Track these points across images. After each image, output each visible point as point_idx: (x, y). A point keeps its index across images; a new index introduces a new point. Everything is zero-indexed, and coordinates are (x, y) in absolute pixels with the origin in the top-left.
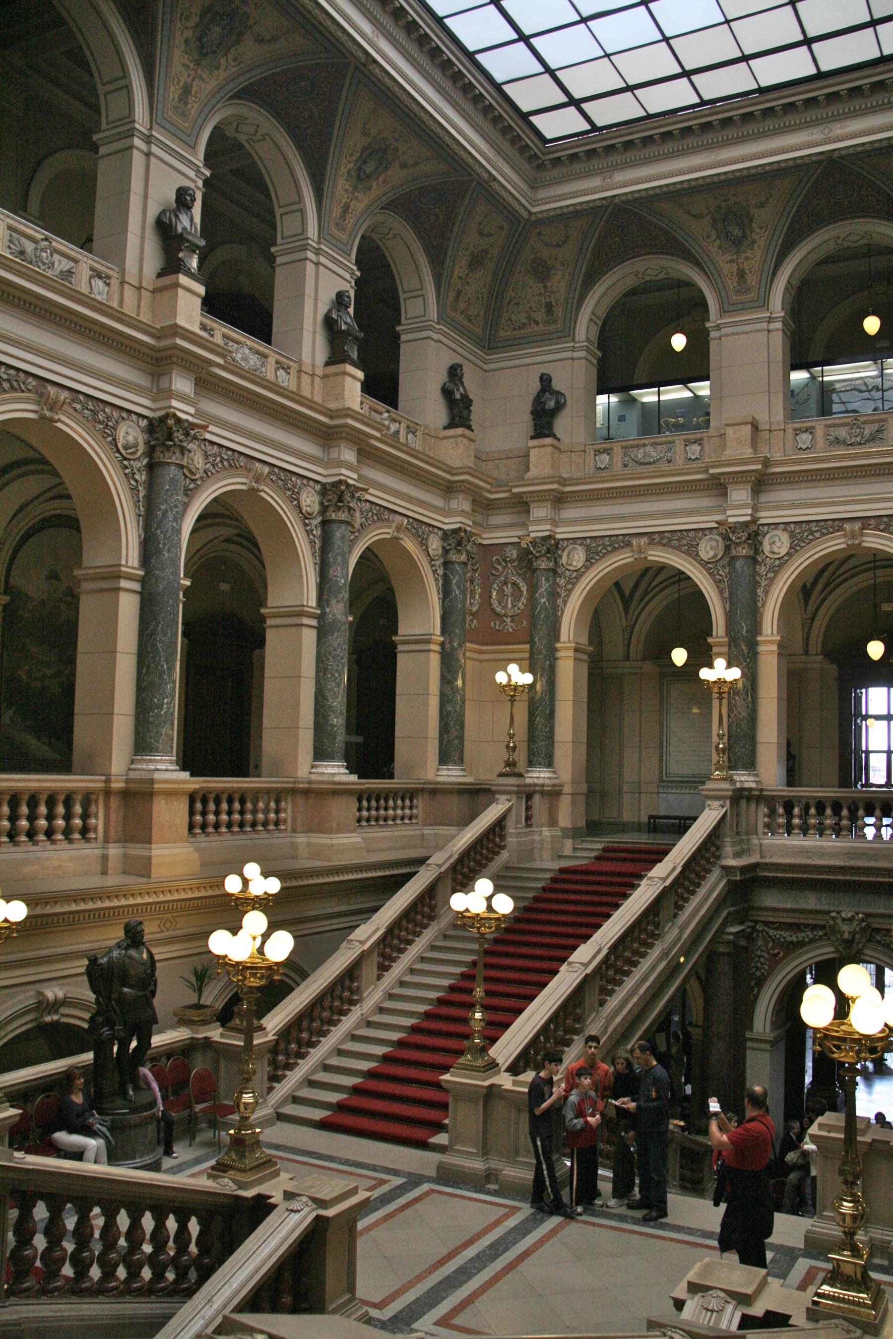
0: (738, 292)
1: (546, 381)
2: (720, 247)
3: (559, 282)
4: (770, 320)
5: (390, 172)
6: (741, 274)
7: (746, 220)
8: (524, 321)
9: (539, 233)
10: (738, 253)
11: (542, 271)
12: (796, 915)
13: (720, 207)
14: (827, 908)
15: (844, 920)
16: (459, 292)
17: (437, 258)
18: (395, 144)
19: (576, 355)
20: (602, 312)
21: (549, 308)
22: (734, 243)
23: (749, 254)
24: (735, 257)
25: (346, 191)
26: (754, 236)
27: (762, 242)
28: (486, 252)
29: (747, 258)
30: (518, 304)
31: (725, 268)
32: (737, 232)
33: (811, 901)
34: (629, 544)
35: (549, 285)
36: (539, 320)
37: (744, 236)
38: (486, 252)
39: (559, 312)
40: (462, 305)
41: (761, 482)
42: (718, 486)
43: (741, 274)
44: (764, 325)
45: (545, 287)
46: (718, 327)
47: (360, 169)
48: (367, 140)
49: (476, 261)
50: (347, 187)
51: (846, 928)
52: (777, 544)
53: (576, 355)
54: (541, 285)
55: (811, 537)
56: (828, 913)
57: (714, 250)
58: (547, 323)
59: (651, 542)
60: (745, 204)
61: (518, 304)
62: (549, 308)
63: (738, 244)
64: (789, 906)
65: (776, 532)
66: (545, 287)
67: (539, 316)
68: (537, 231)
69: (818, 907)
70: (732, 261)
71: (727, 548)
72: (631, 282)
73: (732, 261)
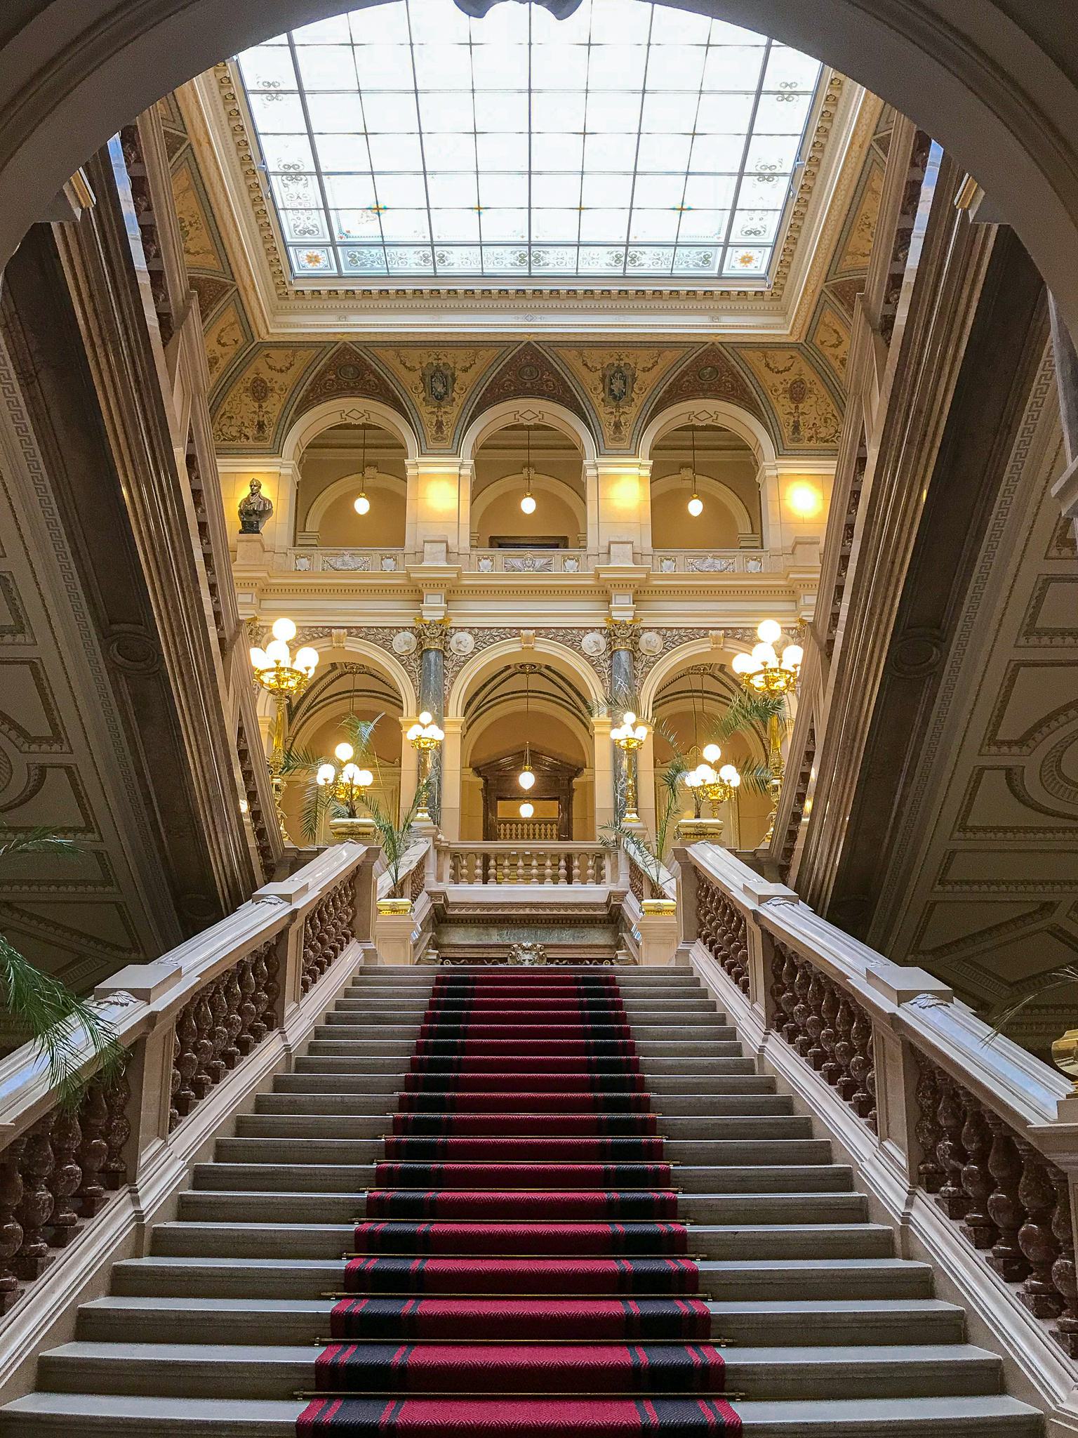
1: (255, 488)
3: (274, 405)
4: (461, 466)
6: (439, 425)
9: (267, 356)
11: (260, 391)
12: (481, 950)
14: (507, 942)
15: (524, 949)
19: (283, 471)
20: (306, 441)
21: (261, 426)
23: (448, 409)
27: (459, 401)
31: (426, 417)
32: (440, 389)
33: (494, 937)
34: (330, 635)
35: (264, 405)
37: (446, 393)
39: (269, 431)
41: (453, 592)
42: (416, 594)
43: (439, 425)
44: (456, 470)
45: (260, 407)
46: (416, 465)
51: (527, 957)
52: (465, 641)
53: (283, 471)
54: (256, 405)
56: (509, 946)
57: (418, 400)
59: (350, 634)
62: (261, 426)
63: (440, 398)
64: (474, 942)
65: (461, 634)
66: (260, 407)
68: (266, 352)
69: (500, 942)
70: (432, 413)
71: (420, 644)
72: (336, 420)
73: (432, 413)
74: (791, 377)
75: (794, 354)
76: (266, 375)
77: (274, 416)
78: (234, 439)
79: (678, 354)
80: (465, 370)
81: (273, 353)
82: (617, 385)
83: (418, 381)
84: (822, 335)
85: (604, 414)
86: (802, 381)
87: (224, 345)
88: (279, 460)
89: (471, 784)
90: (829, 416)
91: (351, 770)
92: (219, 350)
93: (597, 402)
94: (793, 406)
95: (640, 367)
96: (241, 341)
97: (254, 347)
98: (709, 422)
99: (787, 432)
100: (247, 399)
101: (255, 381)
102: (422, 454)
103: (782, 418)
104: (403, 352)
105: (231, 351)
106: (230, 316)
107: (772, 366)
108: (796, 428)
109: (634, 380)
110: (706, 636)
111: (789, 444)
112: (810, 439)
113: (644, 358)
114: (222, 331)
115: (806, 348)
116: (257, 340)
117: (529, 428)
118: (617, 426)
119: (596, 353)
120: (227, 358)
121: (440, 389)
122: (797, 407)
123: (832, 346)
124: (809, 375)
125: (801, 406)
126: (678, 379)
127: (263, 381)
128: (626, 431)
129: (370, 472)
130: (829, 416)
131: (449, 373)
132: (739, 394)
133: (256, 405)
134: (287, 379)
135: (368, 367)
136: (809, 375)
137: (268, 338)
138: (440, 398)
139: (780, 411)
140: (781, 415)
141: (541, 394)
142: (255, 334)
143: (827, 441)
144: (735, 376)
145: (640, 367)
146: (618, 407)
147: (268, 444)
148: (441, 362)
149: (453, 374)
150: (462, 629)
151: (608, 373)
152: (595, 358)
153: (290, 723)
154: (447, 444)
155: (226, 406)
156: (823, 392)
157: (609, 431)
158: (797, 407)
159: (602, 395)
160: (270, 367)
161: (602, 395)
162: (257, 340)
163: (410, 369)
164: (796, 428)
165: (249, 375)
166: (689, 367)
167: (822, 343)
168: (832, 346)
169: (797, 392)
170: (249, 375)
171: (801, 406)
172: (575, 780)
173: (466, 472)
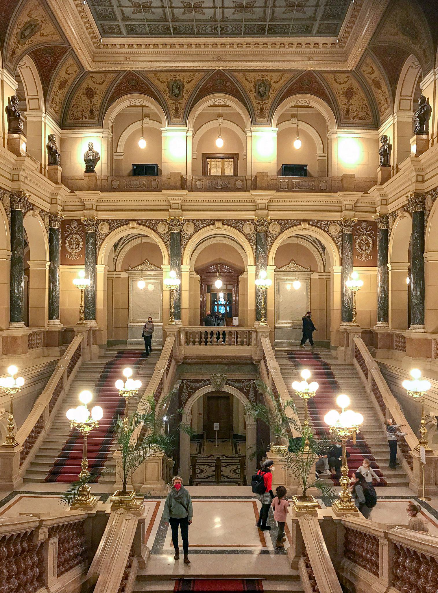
3: (97, 100)
5: (35, 37)
7: (181, 87)
8: (79, 116)
9: (92, 77)
10: (176, 100)
11: (90, 94)
16: (53, 99)
17: (46, 80)
18: (41, 24)
21: (92, 111)
22: (175, 96)
23: (181, 101)
24: (175, 102)
25: (15, 43)
26: (184, 94)
28: (66, 81)
29: (179, 103)
30: (77, 107)
32: (177, 91)
36: (87, 116)
37: (180, 93)
38: (66, 81)
39: (96, 114)
40: (54, 105)
45: (91, 101)
47: (22, 33)
48: (29, 19)
49: (62, 85)
50: (15, 41)
54: (89, 101)
58: (91, 118)
60: (182, 80)
61: (77, 107)
62: (92, 111)
63: (177, 96)
66: (91, 101)
67: (87, 114)
70: (173, 103)
73: (173, 103)
74: (346, 86)
75: (349, 75)
76: (92, 86)
77: (98, 106)
78: (79, 118)
79: (292, 74)
80: (188, 82)
81: (94, 75)
82: (262, 90)
84: (364, 68)
85: (255, 103)
86: (352, 89)
87: (69, 74)
88: (102, 130)
89: (195, 278)
90: (364, 106)
91: (130, 381)
92: (67, 77)
93: (252, 97)
94: (347, 101)
95: (273, 81)
96: (78, 71)
97: (84, 74)
98: (306, 104)
99: (343, 114)
100: (84, 97)
101: (87, 89)
102: (169, 125)
103: (341, 106)
104: (158, 74)
105: (73, 76)
106: (70, 61)
107: (338, 81)
108: (348, 111)
109: (270, 87)
111: (343, 121)
112: (353, 118)
113: (275, 77)
114: (67, 68)
115: (357, 73)
116: (86, 70)
117: (220, 106)
118: (262, 110)
119: (252, 74)
120: (72, 79)
121: (177, 91)
122: (348, 102)
123: (369, 73)
124: (356, 85)
125: (350, 100)
126: (292, 86)
127: (91, 89)
129: (146, 120)
130: (364, 106)
131: (181, 83)
132: (320, 93)
133: (89, 101)
134: (103, 88)
135: (142, 81)
136: (356, 85)
137: (91, 70)
138: (177, 96)
139: (340, 103)
140: (340, 105)
141: (225, 92)
142: (85, 68)
143: (362, 119)
144: (320, 85)
145: (273, 81)
146: (262, 100)
147: (96, 120)
148: (177, 79)
149: (183, 84)
151: (257, 84)
152: (252, 77)
153: (115, 251)
154: (180, 119)
155: (74, 102)
156: (362, 94)
157: (258, 112)
158: (348, 102)
159: (255, 94)
160: (94, 82)
161: (255, 94)
162: (86, 70)
164: (348, 111)
165: (84, 86)
166: (297, 81)
167: (364, 71)
168: (369, 73)
169: (349, 93)
170: (84, 86)
171: (350, 100)
172: (240, 276)
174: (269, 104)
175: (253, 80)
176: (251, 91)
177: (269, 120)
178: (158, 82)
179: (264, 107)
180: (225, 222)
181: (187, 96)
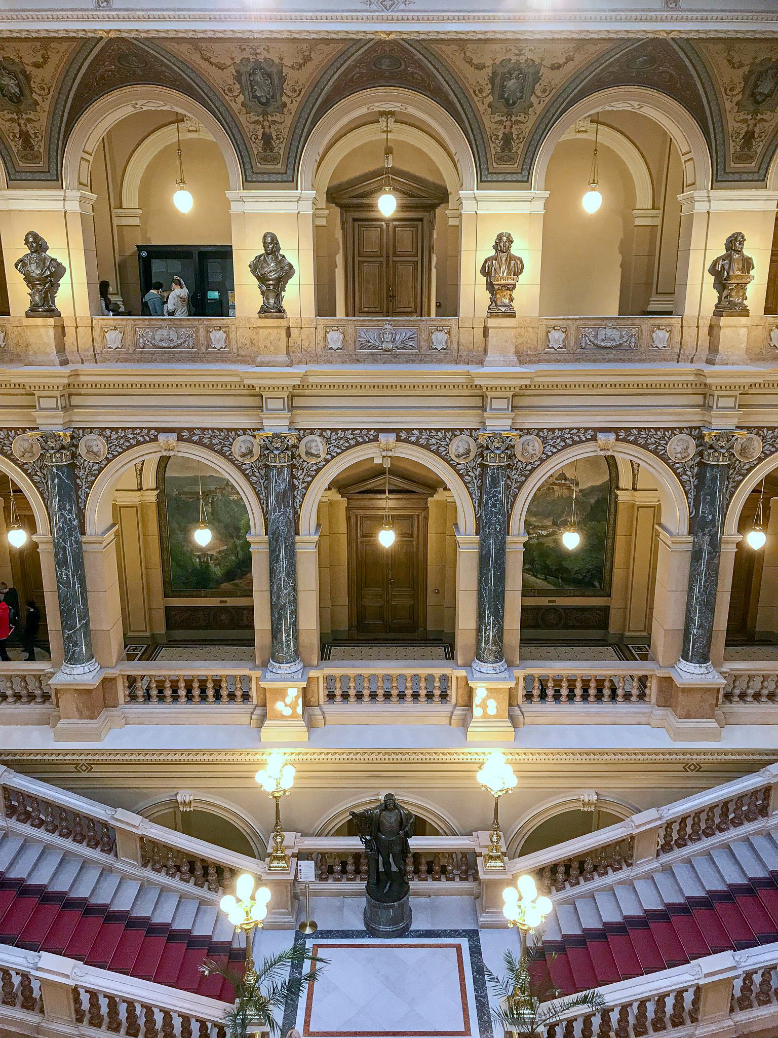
0: (265, 160)
2: (243, 105)
13: (249, 59)
24: (261, 119)
26: (284, 98)
29: (274, 122)
55: (347, 444)
70: (257, 122)
73: (257, 122)
83: (231, 81)
110: (594, 438)
111: (733, 165)
128: (518, 148)
148: (261, 58)
150: (312, 431)
159: (490, 98)
163: (216, 65)
173: (307, 208)
174: (530, 124)
175: (489, 63)
176: (481, 91)
177: (526, 167)
178: (204, 64)
179: (515, 133)
180: (404, 435)
181: (296, 104)
